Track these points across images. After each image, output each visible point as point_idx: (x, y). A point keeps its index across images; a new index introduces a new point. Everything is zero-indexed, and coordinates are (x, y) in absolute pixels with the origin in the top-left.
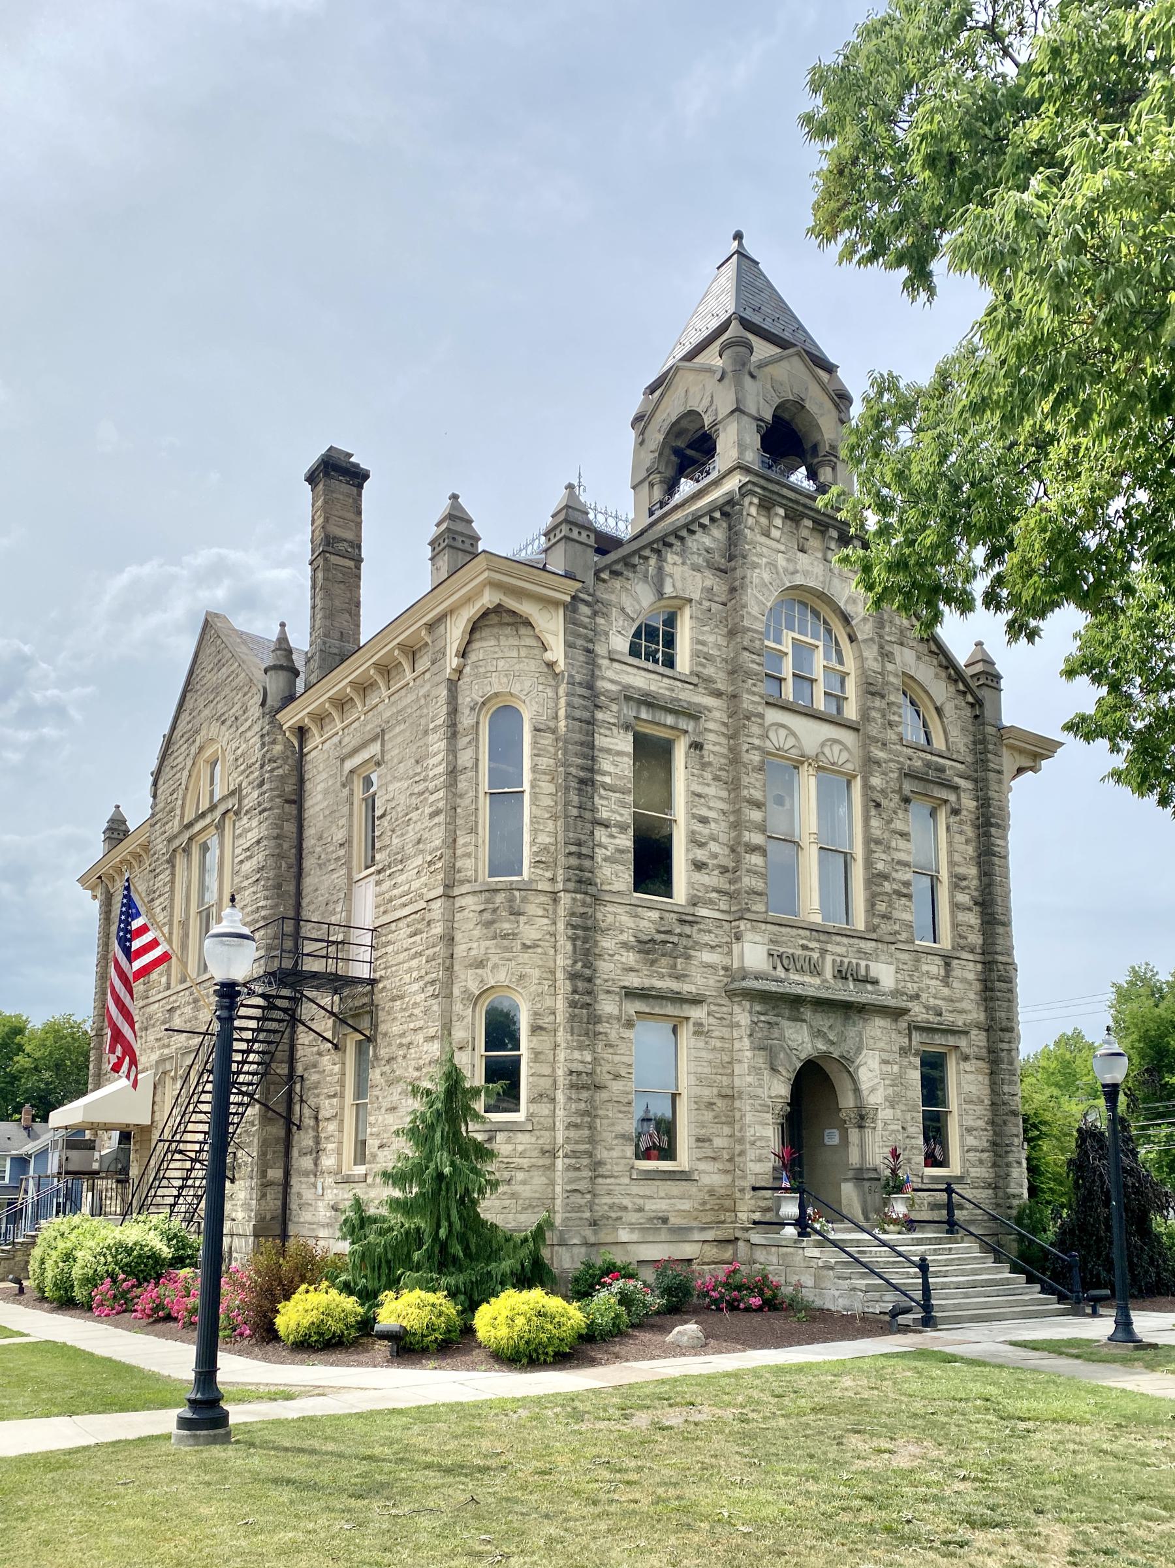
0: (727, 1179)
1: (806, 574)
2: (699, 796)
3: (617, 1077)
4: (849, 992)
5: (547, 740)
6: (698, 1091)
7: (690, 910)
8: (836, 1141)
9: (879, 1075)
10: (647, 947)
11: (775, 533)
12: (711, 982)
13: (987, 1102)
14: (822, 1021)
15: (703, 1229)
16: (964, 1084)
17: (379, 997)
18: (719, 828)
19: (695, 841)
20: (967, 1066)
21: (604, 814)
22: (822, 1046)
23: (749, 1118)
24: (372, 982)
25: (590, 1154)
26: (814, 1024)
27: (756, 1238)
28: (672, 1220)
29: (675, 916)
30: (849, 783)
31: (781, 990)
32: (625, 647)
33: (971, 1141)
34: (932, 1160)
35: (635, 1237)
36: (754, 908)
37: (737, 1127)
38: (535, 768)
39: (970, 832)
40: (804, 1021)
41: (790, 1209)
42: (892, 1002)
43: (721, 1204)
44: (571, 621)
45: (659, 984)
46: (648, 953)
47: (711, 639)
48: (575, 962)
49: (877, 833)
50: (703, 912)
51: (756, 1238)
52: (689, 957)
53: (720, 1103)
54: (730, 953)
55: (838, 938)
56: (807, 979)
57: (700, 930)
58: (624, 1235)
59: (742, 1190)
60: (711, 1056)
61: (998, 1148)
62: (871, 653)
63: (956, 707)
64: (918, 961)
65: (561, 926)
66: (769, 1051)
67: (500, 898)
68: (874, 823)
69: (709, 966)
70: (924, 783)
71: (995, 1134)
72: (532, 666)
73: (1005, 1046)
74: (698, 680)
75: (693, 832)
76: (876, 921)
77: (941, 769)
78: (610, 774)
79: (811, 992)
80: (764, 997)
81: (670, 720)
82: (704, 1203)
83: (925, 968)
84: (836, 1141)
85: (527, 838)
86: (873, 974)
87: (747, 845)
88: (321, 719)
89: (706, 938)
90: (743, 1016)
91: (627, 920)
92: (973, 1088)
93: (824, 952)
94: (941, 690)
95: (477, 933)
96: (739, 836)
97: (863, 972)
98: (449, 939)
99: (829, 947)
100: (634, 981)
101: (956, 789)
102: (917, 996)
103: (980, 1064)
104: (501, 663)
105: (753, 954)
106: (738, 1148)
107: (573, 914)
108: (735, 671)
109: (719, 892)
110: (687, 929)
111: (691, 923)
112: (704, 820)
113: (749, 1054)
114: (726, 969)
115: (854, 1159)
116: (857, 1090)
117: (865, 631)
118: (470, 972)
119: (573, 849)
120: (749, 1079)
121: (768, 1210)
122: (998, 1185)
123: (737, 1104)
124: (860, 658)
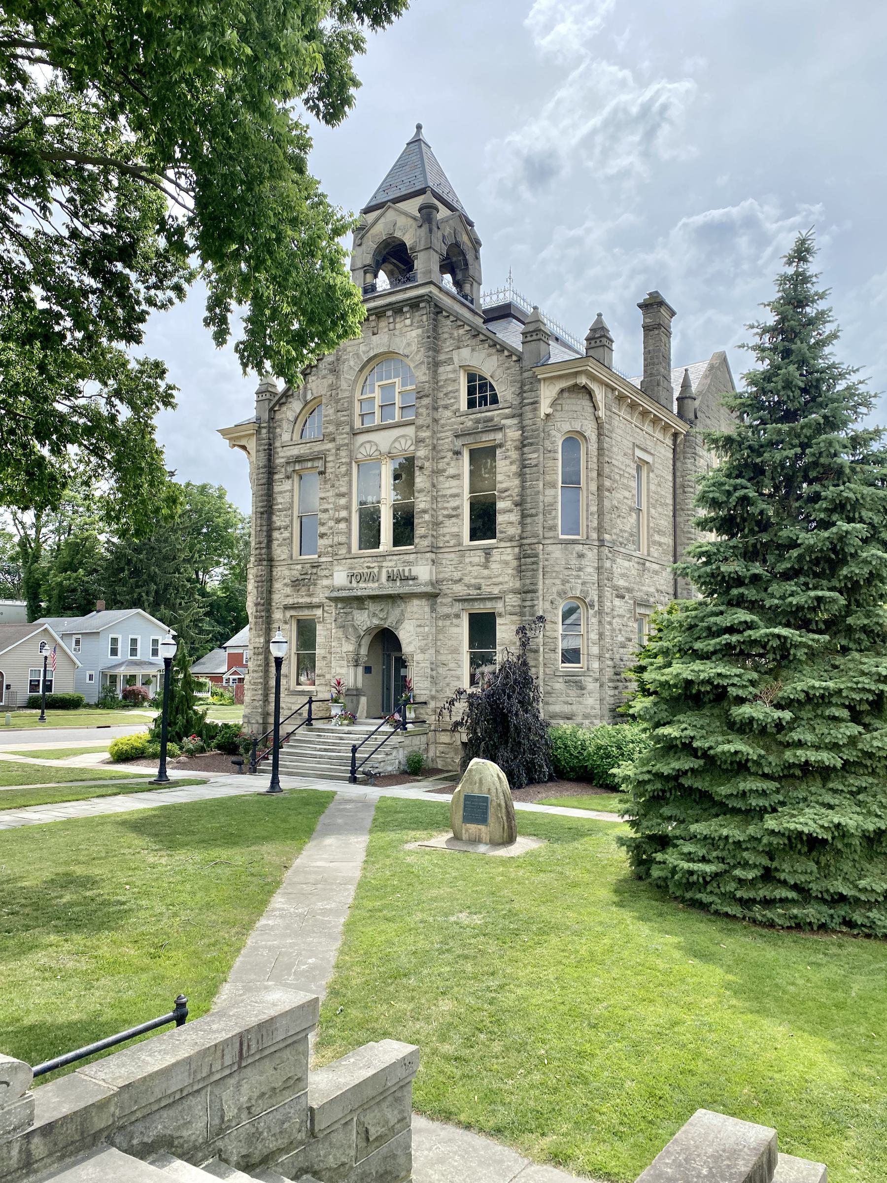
4: (397, 588)
21: (278, 524)
22: (376, 621)
45: (301, 600)
50: (323, 559)
56: (371, 585)
86: (413, 574)
89: (326, 573)
91: (287, 573)
93: (380, 567)
99: (384, 564)
100: (290, 601)
110: (315, 571)
111: (317, 567)
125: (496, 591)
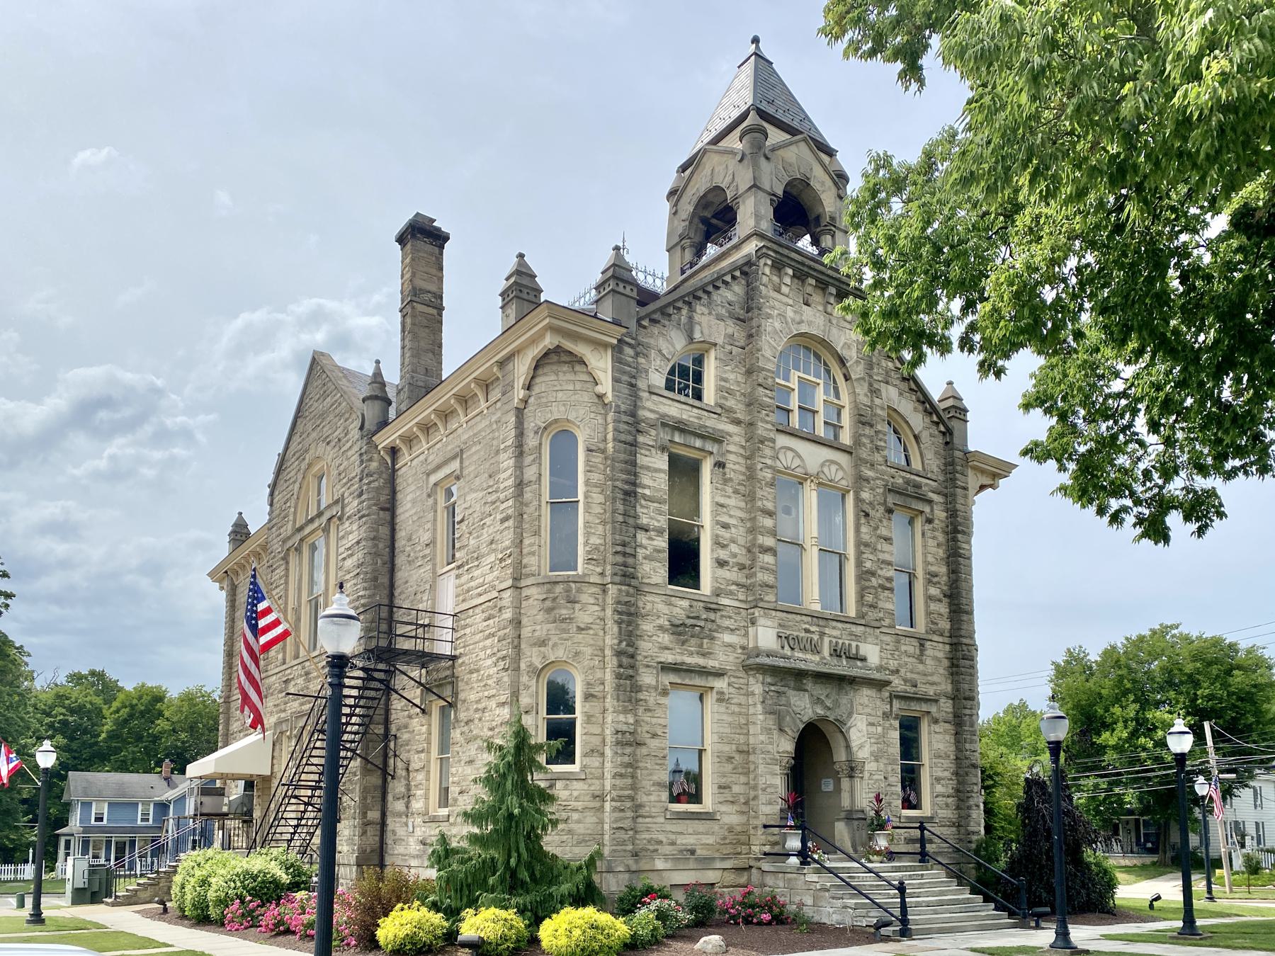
0: (743, 819)
1: (810, 323)
2: (722, 506)
3: (654, 735)
5: (597, 458)
6: (720, 747)
7: (714, 599)
8: (831, 788)
9: (866, 735)
10: (679, 630)
11: (785, 289)
12: (731, 659)
13: (952, 757)
14: (820, 691)
15: (723, 859)
16: (935, 743)
17: (459, 671)
18: (739, 533)
19: (718, 543)
20: (937, 728)
21: (644, 520)
22: (820, 711)
23: (761, 769)
24: (453, 658)
25: (632, 799)
26: (814, 693)
27: (766, 866)
28: (699, 852)
29: (702, 604)
30: (843, 496)
31: (788, 665)
32: (662, 383)
33: (939, 788)
34: (908, 804)
35: (668, 865)
36: (767, 598)
37: (751, 776)
38: (587, 483)
39: (941, 537)
40: (806, 690)
41: (794, 843)
42: (877, 676)
43: (739, 838)
44: (618, 360)
45: (689, 660)
46: (680, 634)
47: (732, 376)
48: (621, 642)
49: (866, 538)
50: (724, 601)
51: (766, 866)
52: (713, 638)
53: (737, 757)
54: (746, 635)
55: (834, 624)
56: (809, 656)
57: (722, 616)
58: (659, 864)
59: (755, 828)
60: (730, 719)
61: (961, 796)
62: (862, 390)
63: (931, 435)
64: (898, 642)
65: (609, 612)
66: (778, 715)
67: (559, 589)
68: (864, 529)
69: (730, 645)
70: (904, 497)
71: (959, 783)
72: (586, 397)
73: (968, 712)
74: (721, 410)
75: (717, 536)
76: (865, 609)
77: (918, 486)
78: (649, 487)
79: (812, 667)
80: (774, 671)
81: (698, 443)
82: (725, 838)
83: (903, 648)
84: (831, 788)
85: (581, 539)
86: (862, 652)
87: (761, 546)
88: (409, 440)
89: (727, 623)
90: (757, 686)
92: (941, 746)
93: (822, 634)
94: (918, 421)
95: (540, 617)
96: (755, 539)
97: (854, 651)
98: (517, 623)
100: (669, 657)
101: (930, 502)
102: (898, 671)
103: (948, 726)
104: (560, 394)
105: (766, 636)
106: (752, 794)
107: (619, 603)
108: (751, 403)
109: (737, 585)
110: (712, 616)
111: (715, 610)
112: (726, 526)
113: (761, 717)
114: (743, 648)
115: (846, 803)
116: (848, 747)
117: (857, 371)
118: (535, 649)
119: (619, 548)
120: (762, 738)
121: (776, 843)
122: (960, 823)
123: (752, 758)
124: (853, 393)
125: (931, 691)
